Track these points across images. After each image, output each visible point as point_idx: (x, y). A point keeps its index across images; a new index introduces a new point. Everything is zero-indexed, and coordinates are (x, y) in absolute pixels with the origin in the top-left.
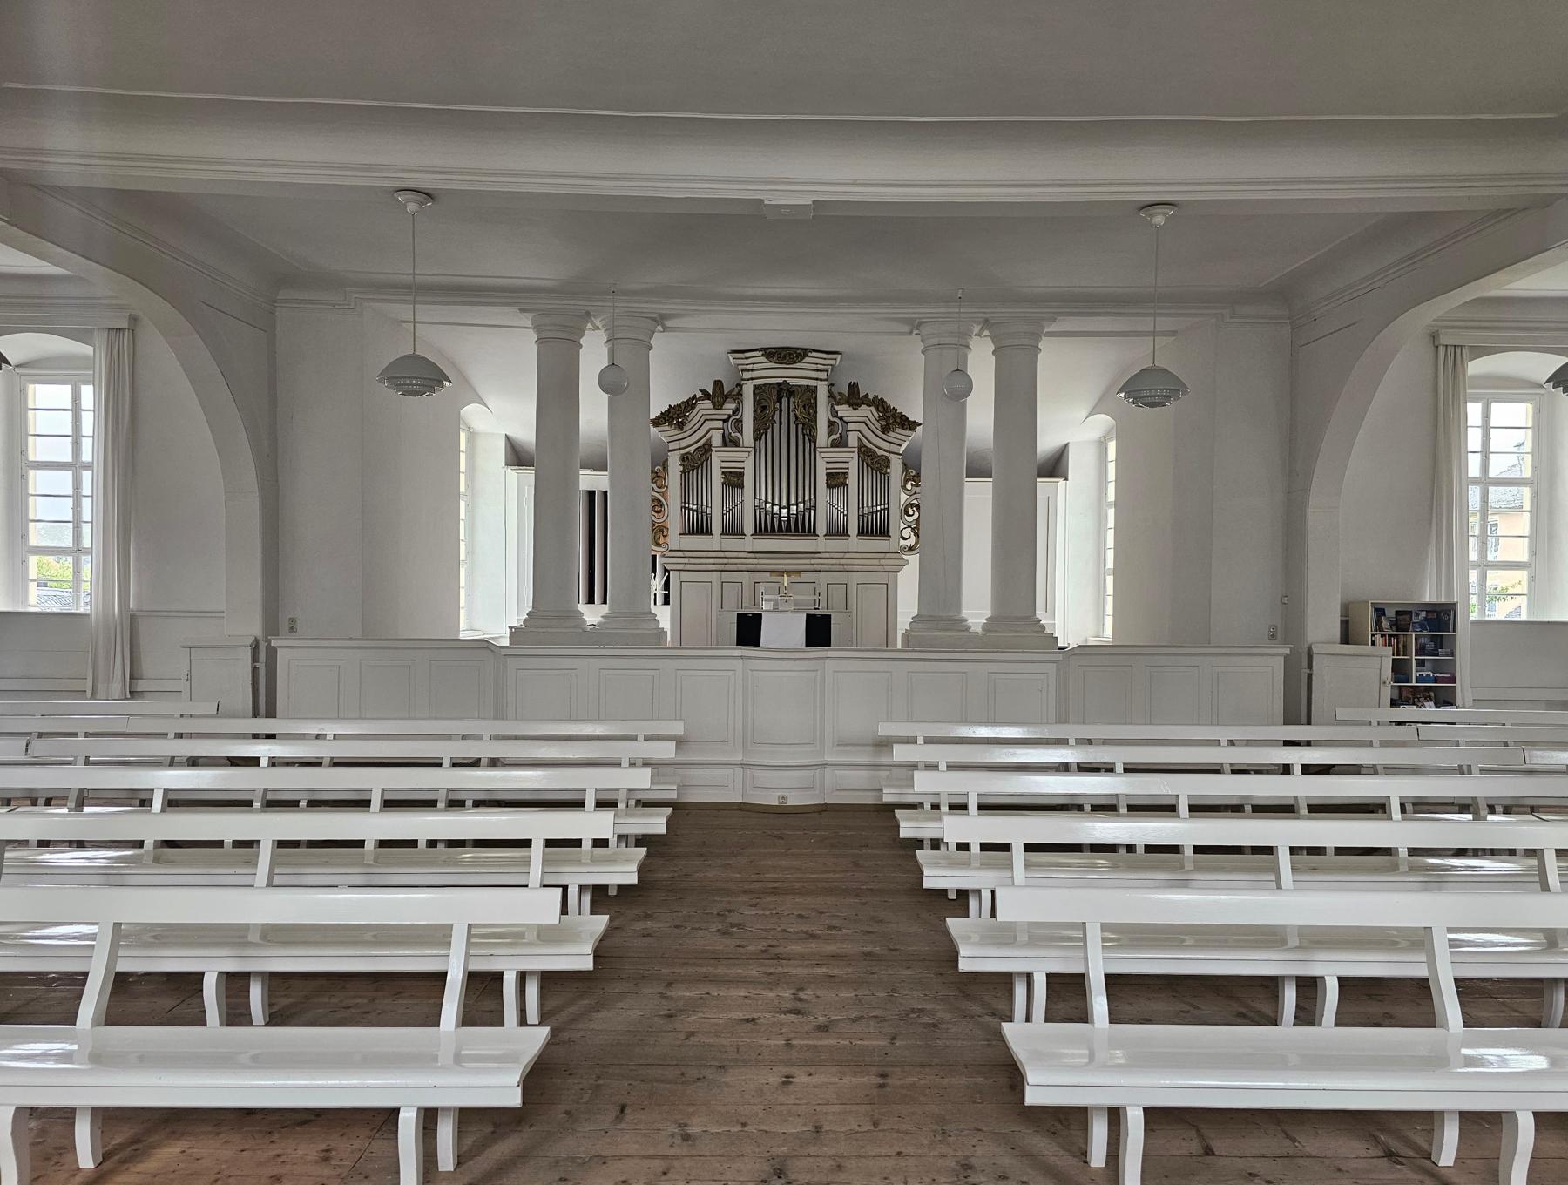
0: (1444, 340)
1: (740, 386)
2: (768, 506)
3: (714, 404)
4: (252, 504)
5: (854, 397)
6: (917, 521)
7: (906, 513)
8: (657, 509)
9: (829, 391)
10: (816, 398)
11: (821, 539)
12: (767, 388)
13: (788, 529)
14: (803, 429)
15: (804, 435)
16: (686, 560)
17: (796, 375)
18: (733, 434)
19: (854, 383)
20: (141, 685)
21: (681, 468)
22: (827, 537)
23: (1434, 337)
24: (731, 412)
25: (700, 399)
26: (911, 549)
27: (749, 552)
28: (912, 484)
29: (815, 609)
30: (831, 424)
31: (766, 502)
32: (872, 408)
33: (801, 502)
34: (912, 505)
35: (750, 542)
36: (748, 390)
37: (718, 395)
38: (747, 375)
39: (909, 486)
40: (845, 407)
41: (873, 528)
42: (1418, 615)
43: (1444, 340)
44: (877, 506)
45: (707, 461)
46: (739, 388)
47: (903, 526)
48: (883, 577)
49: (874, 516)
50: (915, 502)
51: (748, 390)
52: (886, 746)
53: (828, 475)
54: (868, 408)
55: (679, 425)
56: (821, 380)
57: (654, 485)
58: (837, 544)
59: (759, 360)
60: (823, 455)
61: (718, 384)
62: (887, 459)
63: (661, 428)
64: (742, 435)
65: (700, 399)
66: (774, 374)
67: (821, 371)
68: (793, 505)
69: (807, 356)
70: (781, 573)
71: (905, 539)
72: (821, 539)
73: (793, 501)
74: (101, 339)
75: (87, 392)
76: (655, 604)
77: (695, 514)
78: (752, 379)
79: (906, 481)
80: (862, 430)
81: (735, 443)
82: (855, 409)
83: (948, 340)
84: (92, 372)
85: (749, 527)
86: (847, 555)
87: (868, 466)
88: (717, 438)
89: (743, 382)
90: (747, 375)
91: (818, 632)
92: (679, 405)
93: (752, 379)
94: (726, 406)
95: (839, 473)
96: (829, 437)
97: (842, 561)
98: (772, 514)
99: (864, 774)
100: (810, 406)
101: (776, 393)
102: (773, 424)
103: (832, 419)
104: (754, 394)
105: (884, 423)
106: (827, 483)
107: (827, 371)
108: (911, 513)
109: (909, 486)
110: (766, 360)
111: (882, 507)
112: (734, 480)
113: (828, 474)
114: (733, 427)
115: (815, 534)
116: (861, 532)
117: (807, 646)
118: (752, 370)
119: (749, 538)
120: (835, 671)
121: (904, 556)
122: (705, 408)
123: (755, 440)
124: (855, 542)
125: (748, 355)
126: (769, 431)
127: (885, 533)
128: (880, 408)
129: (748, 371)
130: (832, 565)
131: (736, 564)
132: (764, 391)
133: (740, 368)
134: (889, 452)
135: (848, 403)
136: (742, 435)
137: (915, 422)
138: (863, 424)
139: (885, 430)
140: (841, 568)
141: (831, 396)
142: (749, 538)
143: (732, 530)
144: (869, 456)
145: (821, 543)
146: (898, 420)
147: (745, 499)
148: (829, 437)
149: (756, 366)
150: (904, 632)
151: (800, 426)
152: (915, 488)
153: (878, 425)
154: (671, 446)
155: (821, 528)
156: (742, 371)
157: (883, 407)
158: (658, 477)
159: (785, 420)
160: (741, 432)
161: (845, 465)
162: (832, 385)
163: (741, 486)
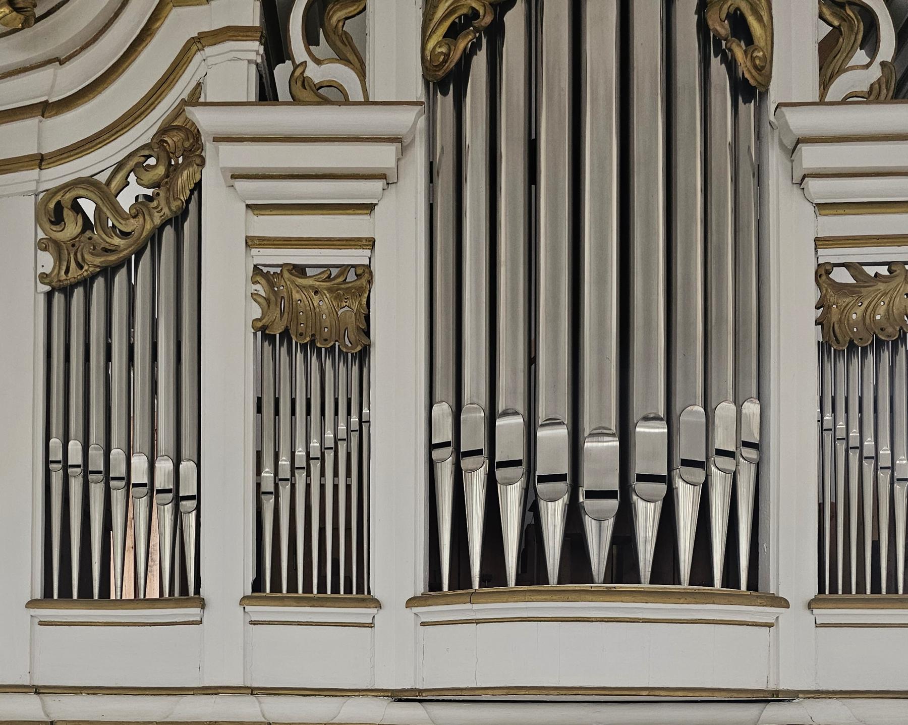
22: (826, 614)
45: (177, 220)
64: (362, 73)
136: (362, 73)
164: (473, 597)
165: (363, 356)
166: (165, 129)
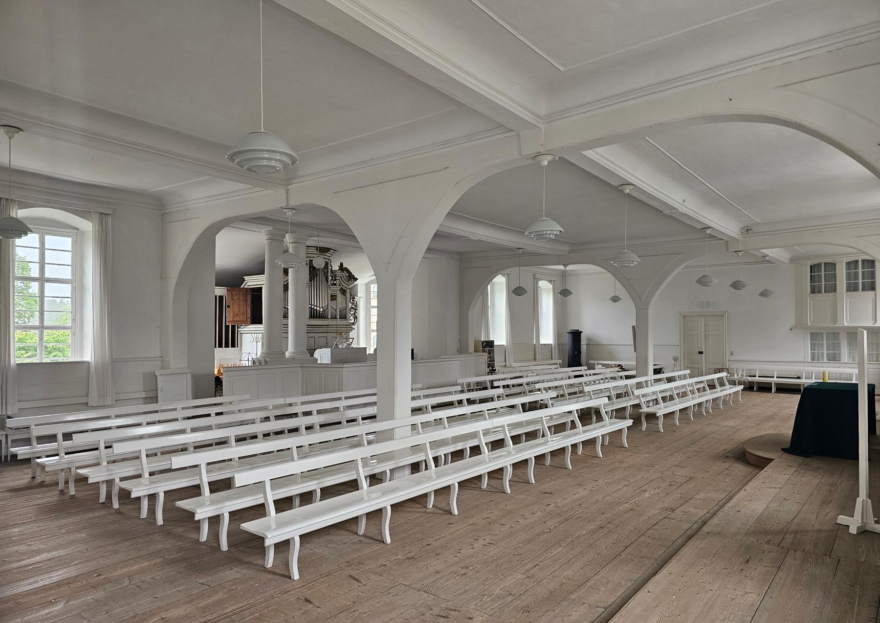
6: (354, 314)
26: (353, 324)
32: (346, 273)
34: (352, 308)
39: (351, 301)
50: (353, 307)
58: (334, 322)
59: (314, 250)
109: (351, 301)
123: (310, 281)
159: (321, 274)
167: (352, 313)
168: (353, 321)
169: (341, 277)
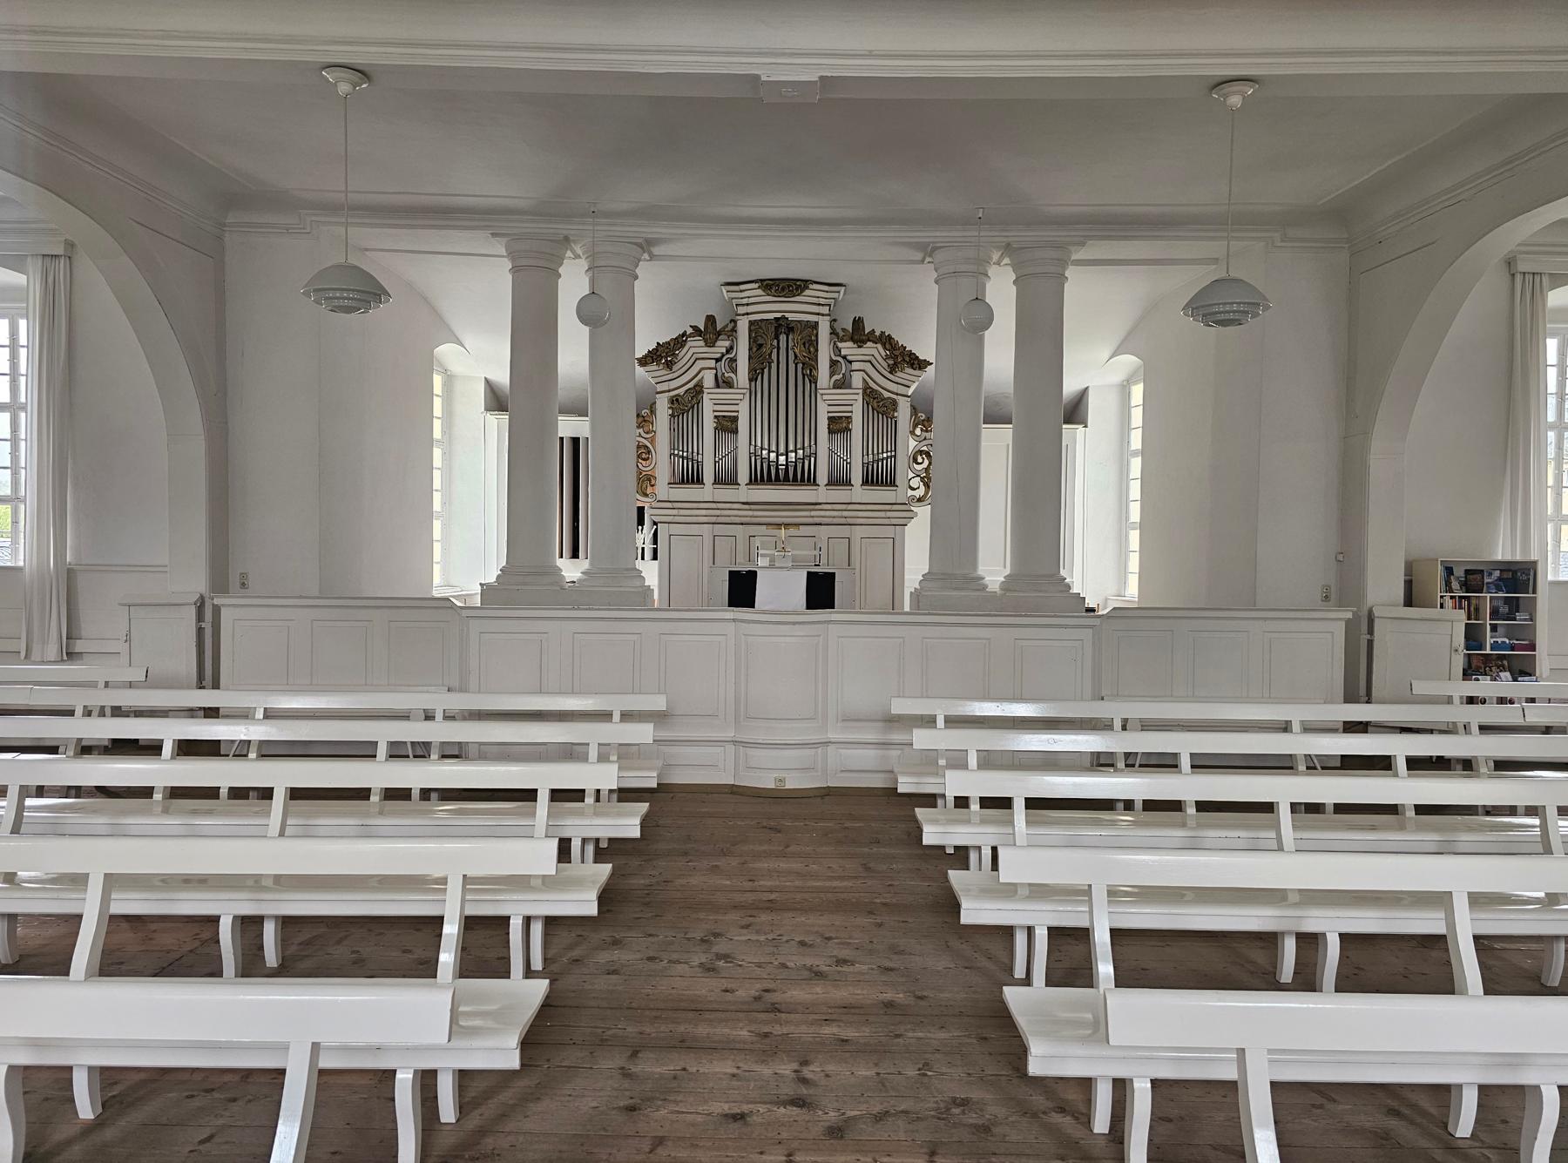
0: (1522, 267)
1: (734, 321)
2: (764, 452)
3: (706, 341)
4: (197, 447)
5: (858, 334)
6: (927, 469)
7: (915, 461)
8: (644, 456)
9: (832, 327)
10: (817, 335)
11: (822, 489)
12: (764, 324)
13: (786, 479)
14: (803, 369)
15: (804, 375)
16: (675, 512)
17: (795, 309)
18: (726, 375)
19: (859, 318)
20: (79, 646)
21: (670, 412)
22: (828, 487)
23: (1510, 263)
24: (724, 350)
25: (690, 336)
26: (920, 500)
27: (744, 503)
28: (922, 430)
29: (815, 565)
30: (833, 363)
31: (762, 449)
32: (879, 346)
33: (800, 449)
34: (921, 452)
35: (745, 493)
36: (743, 326)
37: (710, 331)
38: (741, 310)
39: (918, 431)
40: (850, 344)
41: (878, 477)
42: (1490, 574)
43: (1522, 267)
44: (883, 453)
45: (698, 404)
46: (733, 324)
47: (911, 475)
48: (889, 531)
49: (880, 463)
50: (925, 448)
51: (743, 326)
52: (898, 721)
53: (830, 419)
54: (875, 345)
55: (667, 364)
56: (823, 315)
57: (641, 430)
58: (839, 494)
59: (755, 292)
60: (825, 397)
61: (710, 320)
62: (894, 403)
63: (649, 368)
65: (690, 336)
66: (771, 308)
67: (823, 305)
68: (792, 451)
69: (807, 288)
70: (778, 526)
71: (913, 489)
72: (822, 489)
73: (791, 447)
74: (34, 266)
75: (23, 324)
76: (643, 558)
77: (685, 461)
78: (748, 314)
79: (915, 426)
80: (868, 370)
81: (729, 384)
82: (860, 347)
83: (963, 268)
84: (25, 305)
85: (743, 475)
86: (850, 507)
87: (873, 409)
88: (708, 379)
89: (738, 317)
90: (741, 310)
91: (821, 591)
92: (668, 343)
93: (748, 314)
94: (719, 343)
95: (842, 417)
96: (831, 377)
97: (845, 514)
98: (769, 462)
99: (871, 753)
100: (811, 344)
101: (773, 329)
102: (770, 363)
103: (834, 358)
104: (750, 331)
105: (891, 362)
106: (829, 428)
107: (830, 305)
108: (920, 460)
109: (918, 431)
110: (764, 294)
111: (889, 454)
112: (727, 425)
113: (829, 418)
114: (727, 367)
115: (815, 483)
116: (866, 482)
117: (808, 608)
118: (748, 305)
119: (743, 488)
120: (839, 637)
121: (912, 508)
122: (696, 346)
123: (750, 380)
124: (858, 492)
125: (743, 287)
126: (766, 371)
127: (893, 483)
128: (887, 346)
129: (743, 305)
130: (834, 517)
131: (729, 516)
132: (761, 328)
133: (735, 302)
134: (897, 394)
135: (852, 339)
137: (925, 360)
138: (869, 364)
139: (892, 370)
140: (843, 521)
141: (833, 332)
142: (743, 488)
143: (726, 479)
144: (874, 399)
145: (821, 493)
146: (907, 359)
147: (739, 445)
148: (831, 377)
149: (752, 300)
150: (913, 590)
151: (800, 366)
152: (925, 434)
153: (885, 365)
154: (659, 388)
155: (822, 477)
156: (737, 305)
157: (891, 344)
158: (645, 421)
160: (735, 371)
161: (849, 408)
162: (835, 320)
163: (735, 431)
164: (758, 484)
165: (737, 432)
166: (695, 386)
167: (919, 467)
168: (921, 492)
169: (870, 362)
